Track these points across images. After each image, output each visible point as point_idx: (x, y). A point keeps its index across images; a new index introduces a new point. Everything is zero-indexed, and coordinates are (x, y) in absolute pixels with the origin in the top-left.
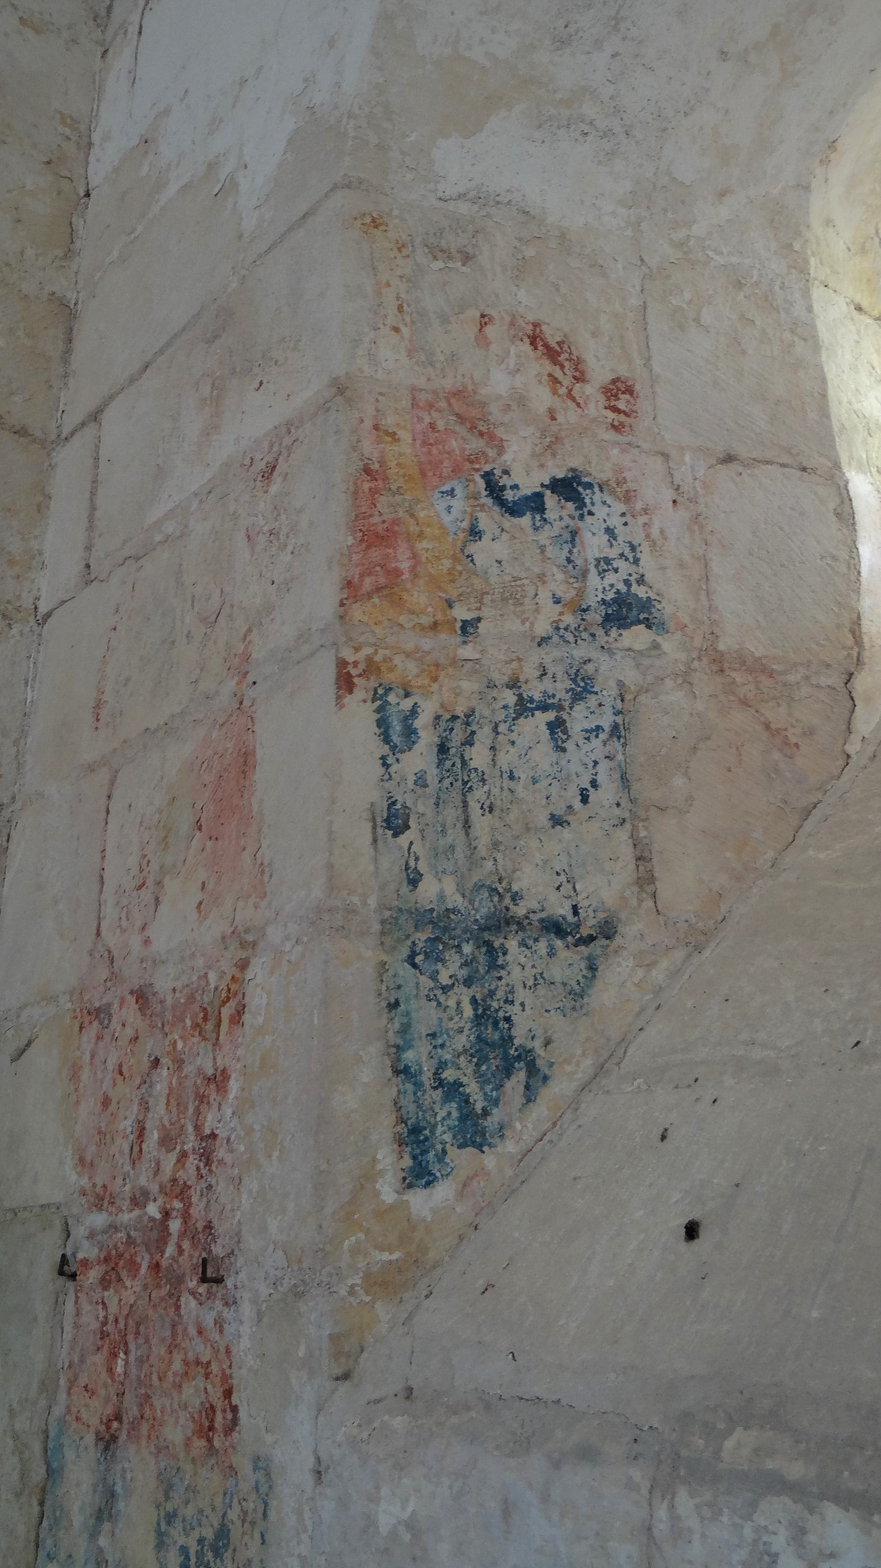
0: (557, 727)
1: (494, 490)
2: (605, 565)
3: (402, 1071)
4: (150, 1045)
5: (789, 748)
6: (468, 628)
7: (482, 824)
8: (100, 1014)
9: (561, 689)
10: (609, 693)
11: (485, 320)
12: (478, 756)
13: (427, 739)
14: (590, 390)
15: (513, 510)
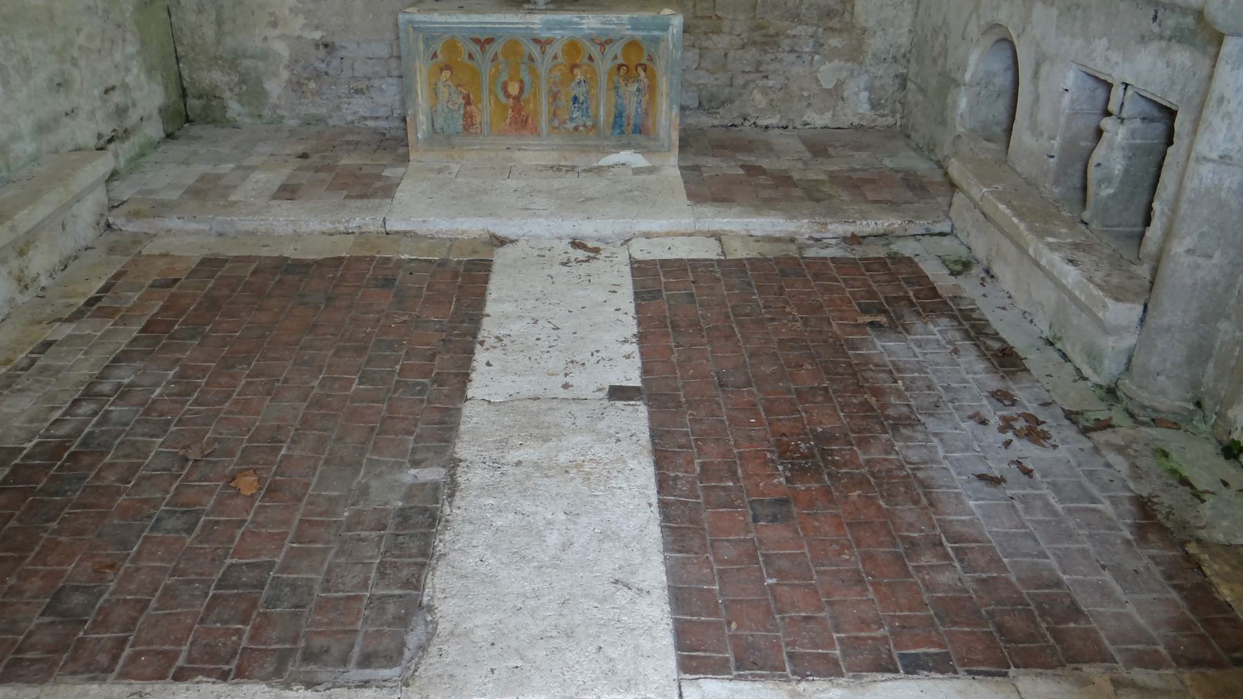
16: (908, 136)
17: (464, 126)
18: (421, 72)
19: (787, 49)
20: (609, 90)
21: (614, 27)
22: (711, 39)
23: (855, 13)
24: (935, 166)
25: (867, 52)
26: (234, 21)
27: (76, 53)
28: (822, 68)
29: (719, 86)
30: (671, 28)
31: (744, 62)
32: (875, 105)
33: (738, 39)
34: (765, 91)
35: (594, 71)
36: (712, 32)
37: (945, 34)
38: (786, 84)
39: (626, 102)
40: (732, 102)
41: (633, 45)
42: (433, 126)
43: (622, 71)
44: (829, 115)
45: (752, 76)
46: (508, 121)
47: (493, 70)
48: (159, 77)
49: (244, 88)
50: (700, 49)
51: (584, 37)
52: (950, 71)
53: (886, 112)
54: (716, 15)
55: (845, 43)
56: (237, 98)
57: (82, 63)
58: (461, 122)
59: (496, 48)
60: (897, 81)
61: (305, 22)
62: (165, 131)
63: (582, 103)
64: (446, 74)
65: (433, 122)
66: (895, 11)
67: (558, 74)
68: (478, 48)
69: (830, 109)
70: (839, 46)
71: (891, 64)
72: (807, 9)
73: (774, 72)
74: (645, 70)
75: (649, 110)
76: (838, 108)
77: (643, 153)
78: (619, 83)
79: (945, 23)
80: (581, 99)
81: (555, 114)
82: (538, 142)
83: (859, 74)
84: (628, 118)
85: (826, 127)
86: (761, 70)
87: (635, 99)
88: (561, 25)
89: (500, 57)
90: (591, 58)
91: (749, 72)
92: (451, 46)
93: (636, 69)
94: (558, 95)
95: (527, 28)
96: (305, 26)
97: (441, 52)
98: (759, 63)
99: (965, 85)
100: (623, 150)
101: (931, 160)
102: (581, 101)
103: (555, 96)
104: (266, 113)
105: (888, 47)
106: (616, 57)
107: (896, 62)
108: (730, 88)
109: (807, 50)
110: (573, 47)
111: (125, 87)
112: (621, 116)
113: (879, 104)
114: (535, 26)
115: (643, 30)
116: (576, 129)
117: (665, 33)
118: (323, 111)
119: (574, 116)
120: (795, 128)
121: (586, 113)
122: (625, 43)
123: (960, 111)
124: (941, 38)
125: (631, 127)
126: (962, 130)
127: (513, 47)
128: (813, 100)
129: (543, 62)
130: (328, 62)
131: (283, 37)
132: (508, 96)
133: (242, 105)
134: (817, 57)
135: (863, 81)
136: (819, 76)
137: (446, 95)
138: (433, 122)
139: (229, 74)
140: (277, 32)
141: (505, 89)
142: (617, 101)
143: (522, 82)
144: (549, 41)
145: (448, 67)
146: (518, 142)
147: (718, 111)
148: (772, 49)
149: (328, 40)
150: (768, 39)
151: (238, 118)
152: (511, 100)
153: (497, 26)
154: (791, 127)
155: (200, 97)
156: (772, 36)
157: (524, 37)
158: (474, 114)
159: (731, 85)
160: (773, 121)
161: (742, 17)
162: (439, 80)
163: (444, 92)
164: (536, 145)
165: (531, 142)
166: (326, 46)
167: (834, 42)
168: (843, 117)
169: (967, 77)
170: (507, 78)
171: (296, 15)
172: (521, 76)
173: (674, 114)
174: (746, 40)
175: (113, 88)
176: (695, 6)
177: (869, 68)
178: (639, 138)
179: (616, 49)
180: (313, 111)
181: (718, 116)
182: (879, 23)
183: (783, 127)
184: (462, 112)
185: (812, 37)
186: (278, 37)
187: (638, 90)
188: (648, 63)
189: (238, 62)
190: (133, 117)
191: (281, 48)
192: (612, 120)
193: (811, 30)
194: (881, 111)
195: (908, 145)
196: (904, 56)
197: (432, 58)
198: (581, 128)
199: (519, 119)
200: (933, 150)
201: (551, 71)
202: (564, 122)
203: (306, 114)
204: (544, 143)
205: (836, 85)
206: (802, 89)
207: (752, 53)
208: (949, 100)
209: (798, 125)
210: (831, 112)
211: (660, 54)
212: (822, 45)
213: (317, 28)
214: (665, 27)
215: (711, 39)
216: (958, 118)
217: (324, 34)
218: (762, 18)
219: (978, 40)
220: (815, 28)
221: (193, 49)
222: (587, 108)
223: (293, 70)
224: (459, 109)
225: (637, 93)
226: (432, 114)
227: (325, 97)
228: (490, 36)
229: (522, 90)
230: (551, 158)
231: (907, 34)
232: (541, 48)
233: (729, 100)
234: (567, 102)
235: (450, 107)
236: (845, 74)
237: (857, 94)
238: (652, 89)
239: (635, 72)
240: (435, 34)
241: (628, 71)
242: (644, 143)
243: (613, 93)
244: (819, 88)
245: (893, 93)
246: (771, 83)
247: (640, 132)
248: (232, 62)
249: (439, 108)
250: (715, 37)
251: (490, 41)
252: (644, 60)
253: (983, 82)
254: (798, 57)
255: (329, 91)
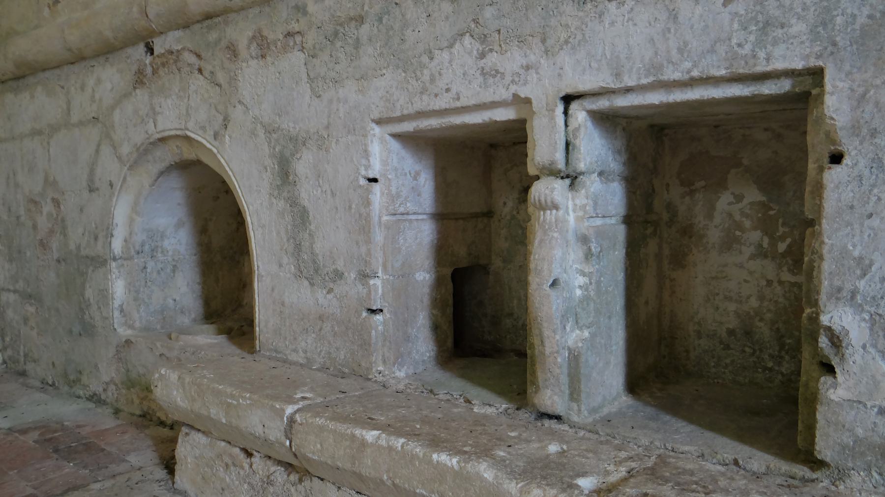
16: (23, 374)
24: (91, 405)
37: (53, 199)
52: (78, 248)
79: (50, 183)
99: (115, 259)
101: (79, 397)
123: (117, 303)
124: (48, 207)
126: (129, 332)
169: (117, 245)
195: (28, 386)
200: (78, 381)
208: (89, 293)
216: (116, 314)
219: (125, 179)
253: (147, 248)
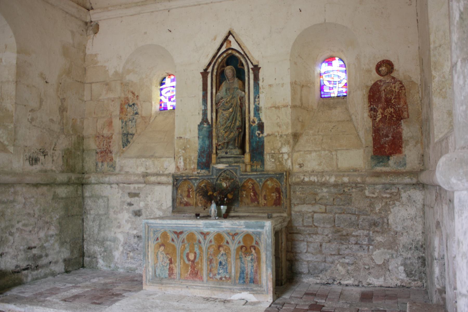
0: (132, 122)
1: (129, 105)
2: (135, 110)
3: (123, 142)
4: (104, 139)
5: (146, 123)
6: (127, 115)
7: (127, 128)
8: (98, 137)
9: (132, 119)
10: (135, 119)
11: (129, 91)
12: (127, 124)
13: (124, 123)
14: (135, 97)
15: (130, 106)
17: (169, 274)
18: (151, 246)
19: (353, 242)
20: (236, 259)
21: (237, 227)
22: (312, 237)
23: (390, 223)
25: (399, 244)
26: (105, 225)
27: (14, 230)
28: (375, 253)
29: (318, 262)
30: (265, 227)
31: (331, 249)
32: (409, 274)
33: (327, 238)
34: (343, 265)
35: (229, 249)
36: (313, 234)
38: (355, 262)
39: (246, 266)
40: (326, 271)
41: (248, 237)
42: (155, 273)
43: (243, 249)
44: (382, 279)
45: (336, 257)
46: (189, 273)
47: (183, 247)
48: (68, 246)
49: (105, 253)
50: (307, 242)
51: (224, 232)
53: (416, 278)
54: (314, 225)
55: (386, 239)
56: (102, 258)
57: (17, 235)
58: (167, 272)
59: (184, 236)
60: (420, 261)
61: (130, 226)
62: (65, 269)
63: (224, 266)
64: (162, 248)
65: (155, 271)
66: (412, 222)
67: (212, 250)
68: (176, 236)
69: (382, 276)
70: (383, 241)
71: (415, 251)
72: (362, 221)
73: (348, 255)
74: (255, 249)
75: (257, 270)
76: (387, 275)
77: (253, 294)
78: (242, 255)
80: (224, 263)
81: (211, 271)
82: (202, 285)
83: (396, 257)
84: (247, 274)
85: (381, 286)
86: (341, 253)
87: (250, 264)
88: (212, 226)
89: (186, 241)
90: (227, 242)
91: (334, 255)
92: (165, 235)
93: (250, 249)
94: (212, 261)
95: (197, 227)
96: (130, 228)
97: (160, 237)
98: (339, 250)
99: (436, 259)
100: (243, 292)
102: (223, 264)
103: (210, 261)
104: (112, 265)
105: (411, 242)
106: (239, 242)
107: (417, 250)
108: (324, 263)
109: (365, 243)
110: (219, 237)
111: (42, 247)
112: (243, 273)
113: (412, 274)
114: (200, 226)
115: (252, 228)
116: (221, 279)
117: (263, 230)
118: (134, 266)
119: (220, 272)
120: (363, 286)
121: (226, 271)
122: (244, 235)
125: (249, 279)
127: (191, 237)
128: (371, 270)
129: (204, 244)
130: (138, 244)
131: (122, 232)
132: (189, 260)
133: (104, 261)
134: (371, 247)
135: (400, 260)
136: (373, 257)
137: (162, 259)
138: (155, 271)
139: (101, 248)
140: (120, 230)
141: (187, 256)
142: (241, 265)
143: (195, 253)
144: (208, 234)
145: (162, 245)
146: (193, 284)
147: (319, 275)
148: (346, 242)
149: (139, 234)
150: (343, 237)
151: (101, 267)
152: (190, 263)
153: (183, 226)
154: (360, 285)
155: (89, 257)
156: (344, 236)
157: (196, 231)
158: (173, 269)
159: (325, 261)
160: (350, 282)
161: (328, 226)
162: (159, 251)
163: (160, 256)
164: (201, 286)
165: (199, 285)
166: (138, 237)
167: (379, 239)
168: (391, 281)
170: (188, 251)
171: (128, 223)
172: (195, 251)
173: (269, 273)
174: (331, 238)
175: (35, 247)
176: (303, 221)
177: (402, 253)
178: (253, 286)
179: (239, 238)
180: (130, 266)
181: (319, 278)
182: (403, 228)
183: (356, 285)
184: (168, 267)
185: (366, 236)
186: (120, 232)
187: (252, 260)
188: (256, 245)
189: (104, 242)
190: (44, 261)
191: (121, 237)
192: (238, 275)
193: (366, 232)
194: (413, 278)
196: (422, 246)
197: (156, 240)
198: (224, 279)
199: (194, 272)
201: (209, 248)
202: (215, 275)
203: (127, 267)
204: (205, 285)
205: (384, 262)
206: (364, 264)
207: (334, 245)
209: (364, 284)
210: (383, 278)
211: (262, 241)
212: (373, 240)
213: (135, 229)
214: (262, 227)
215: (312, 237)
217: (138, 232)
218: (339, 227)
220: (368, 232)
221: (89, 236)
222: (226, 268)
223: (124, 247)
224: (167, 266)
225: (251, 261)
226: (155, 267)
227: (135, 260)
228: (182, 231)
229: (195, 257)
230: (206, 293)
231: (421, 234)
232: (204, 237)
233: (325, 270)
234: (217, 264)
235: (163, 264)
236: (388, 256)
237: (397, 268)
238: (259, 259)
239: (250, 250)
240: (158, 229)
241: (246, 249)
242: (255, 289)
243: (239, 261)
244: (374, 264)
245: (419, 268)
246: (347, 261)
247: (253, 282)
248: (102, 242)
249: (158, 265)
250: (314, 236)
251: (181, 233)
252: (254, 244)
254: (361, 247)
255: (137, 257)
